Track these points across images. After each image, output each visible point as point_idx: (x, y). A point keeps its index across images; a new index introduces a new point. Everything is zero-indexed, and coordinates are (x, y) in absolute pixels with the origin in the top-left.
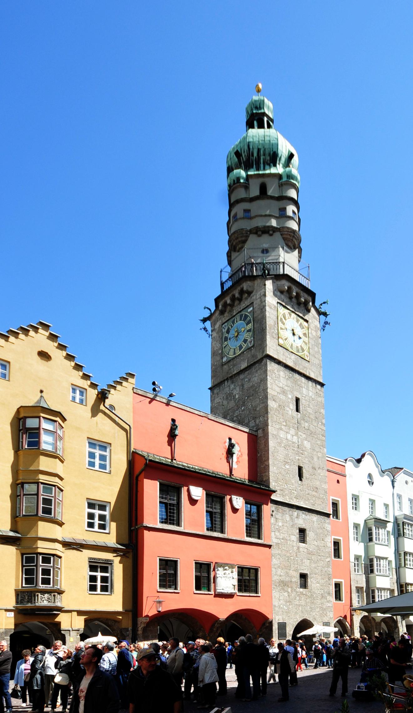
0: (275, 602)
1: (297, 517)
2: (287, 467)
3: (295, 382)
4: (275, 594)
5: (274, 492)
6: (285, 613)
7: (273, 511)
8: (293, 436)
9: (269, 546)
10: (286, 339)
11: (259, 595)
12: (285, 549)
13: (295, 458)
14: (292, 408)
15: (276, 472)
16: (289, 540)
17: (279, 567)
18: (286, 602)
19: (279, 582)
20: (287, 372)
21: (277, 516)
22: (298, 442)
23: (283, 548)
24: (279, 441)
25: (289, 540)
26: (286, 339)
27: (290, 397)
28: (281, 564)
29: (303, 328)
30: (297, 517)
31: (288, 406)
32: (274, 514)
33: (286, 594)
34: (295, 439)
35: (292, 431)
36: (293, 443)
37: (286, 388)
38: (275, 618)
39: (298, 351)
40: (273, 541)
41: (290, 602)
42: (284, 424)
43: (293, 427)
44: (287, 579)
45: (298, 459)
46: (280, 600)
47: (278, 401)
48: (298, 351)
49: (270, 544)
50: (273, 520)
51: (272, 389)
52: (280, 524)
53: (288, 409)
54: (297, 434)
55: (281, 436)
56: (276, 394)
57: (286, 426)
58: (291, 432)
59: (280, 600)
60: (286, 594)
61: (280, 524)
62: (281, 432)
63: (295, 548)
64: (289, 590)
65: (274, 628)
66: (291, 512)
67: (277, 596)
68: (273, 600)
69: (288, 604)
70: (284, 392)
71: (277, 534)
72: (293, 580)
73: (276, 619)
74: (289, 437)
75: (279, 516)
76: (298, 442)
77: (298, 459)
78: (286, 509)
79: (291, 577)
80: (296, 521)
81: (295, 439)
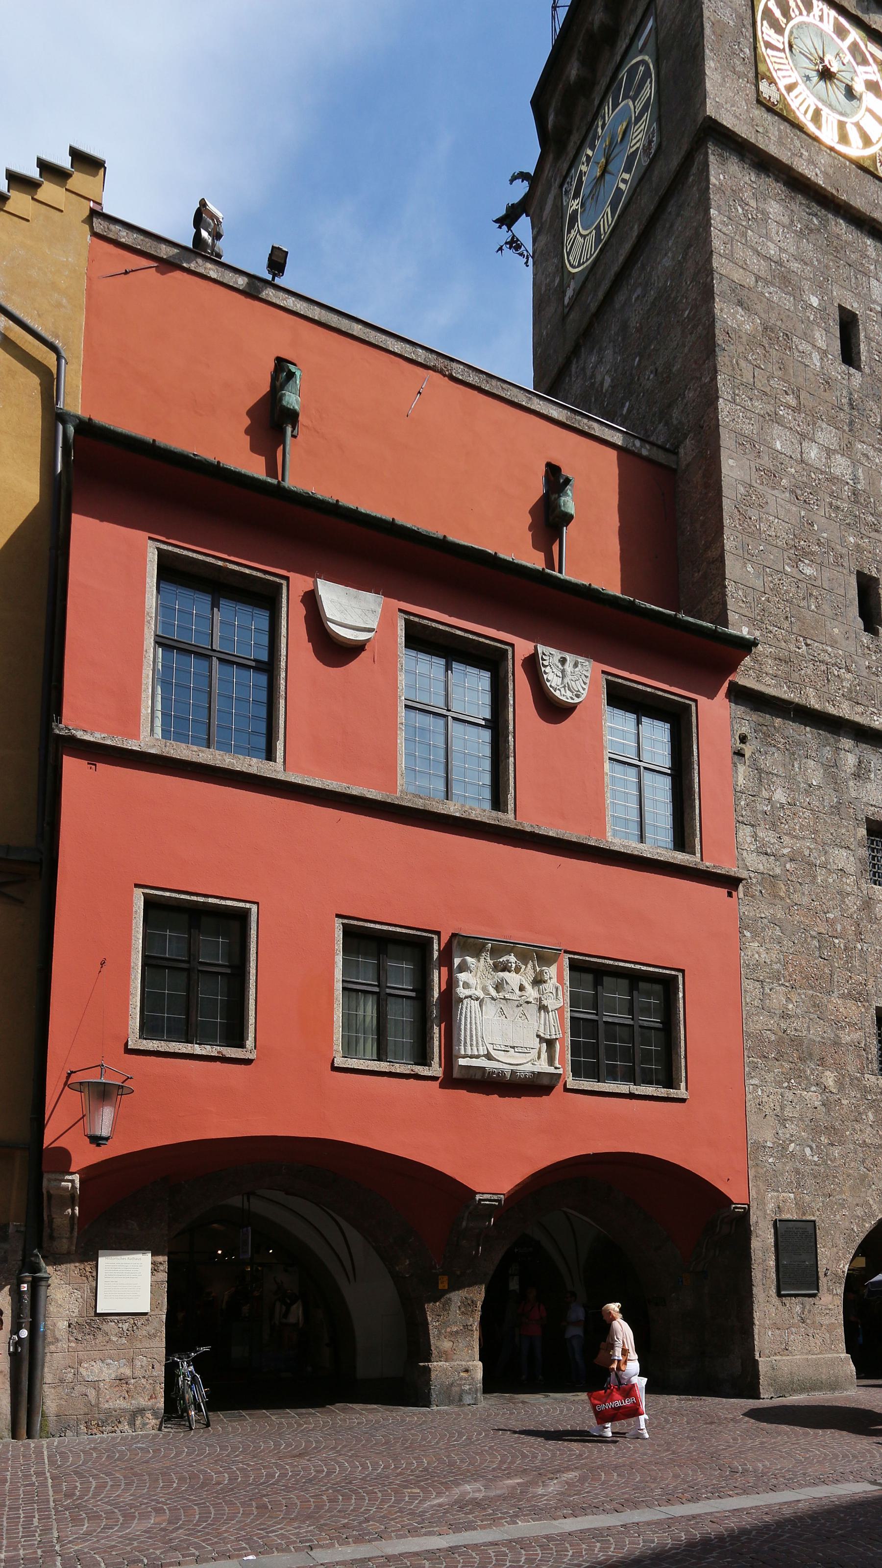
0: (764, 1133)
1: (857, 776)
2: (808, 571)
3: (836, 249)
4: (763, 1089)
5: (746, 646)
6: (810, 1181)
7: (743, 739)
8: (829, 452)
9: (730, 883)
10: (790, 88)
11: (682, 1092)
12: (805, 900)
13: (843, 539)
14: (821, 343)
15: (758, 584)
16: (823, 866)
17: (776, 977)
18: (816, 1129)
19: (780, 1042)
20: (799, 207)
21: (766, 763)
22: (855, 479)
23: (796, 897)
24: (766, 461)
25: (823, 866)
26: (790, 88)
27: (815, 301)
28: (785, 965)
29: (864, 62)
30: (857, 776)
31: (807, 337)
32: (748, 750)
33: (813, 1097)
34: (841, 466)
35: (827, 435)
36: (833, 479)
37: (795, 266)
38: (762, 1203)
39: (844, 138)
40: (749, 862)
41: (830, 1130)
42: (791, 400)
43: (832, 422)
44: (816, 1032)
45: (857, 546)
46: (783, 1121)
47: (758, 307)
48: (844, 138)
49: (733, 871)
50: (742, 774)
51: (730, 258)
52: (780, 796)
53: (804, 346)
54: (847, 450)
55: (778, 446)
56: (750, 281)
57: (796, 410)
58: (820, 436)
59: (783, 1121)
60: (813, 1097)
61: (780, 796)
62: (777, 430)
63: (853, 904)
64: (830, 1079)
65: (755, 1244)
66: (827, 752)
67: (771, 1104)
68: (752, 1118)
69: (824, 1139)
70: (785, 280)
71: (767, 835)
72: (846, 1037)
73: (767, 1206)
74: (813, 453)
75: (773, 761)
76: (855, 479)
77: (857, 546)
78: (808, 734)
79: (838, 1024)
80: (853, 789)
81: (841, 466)
